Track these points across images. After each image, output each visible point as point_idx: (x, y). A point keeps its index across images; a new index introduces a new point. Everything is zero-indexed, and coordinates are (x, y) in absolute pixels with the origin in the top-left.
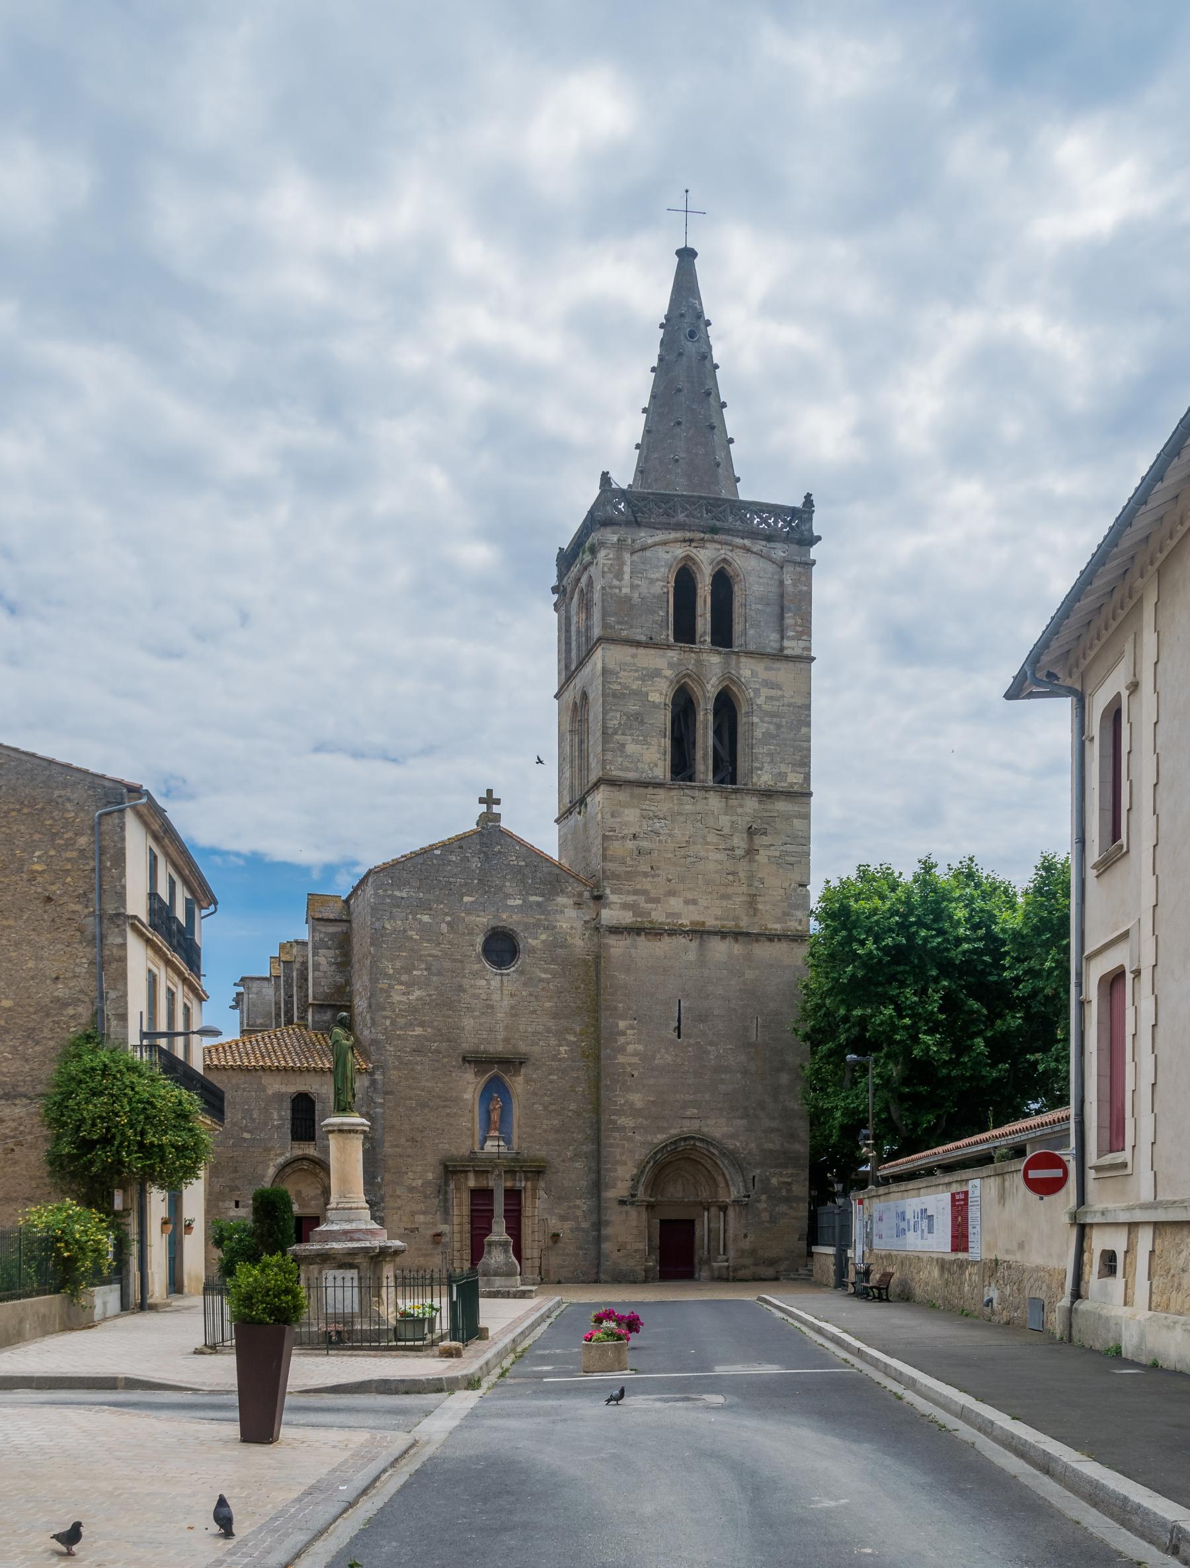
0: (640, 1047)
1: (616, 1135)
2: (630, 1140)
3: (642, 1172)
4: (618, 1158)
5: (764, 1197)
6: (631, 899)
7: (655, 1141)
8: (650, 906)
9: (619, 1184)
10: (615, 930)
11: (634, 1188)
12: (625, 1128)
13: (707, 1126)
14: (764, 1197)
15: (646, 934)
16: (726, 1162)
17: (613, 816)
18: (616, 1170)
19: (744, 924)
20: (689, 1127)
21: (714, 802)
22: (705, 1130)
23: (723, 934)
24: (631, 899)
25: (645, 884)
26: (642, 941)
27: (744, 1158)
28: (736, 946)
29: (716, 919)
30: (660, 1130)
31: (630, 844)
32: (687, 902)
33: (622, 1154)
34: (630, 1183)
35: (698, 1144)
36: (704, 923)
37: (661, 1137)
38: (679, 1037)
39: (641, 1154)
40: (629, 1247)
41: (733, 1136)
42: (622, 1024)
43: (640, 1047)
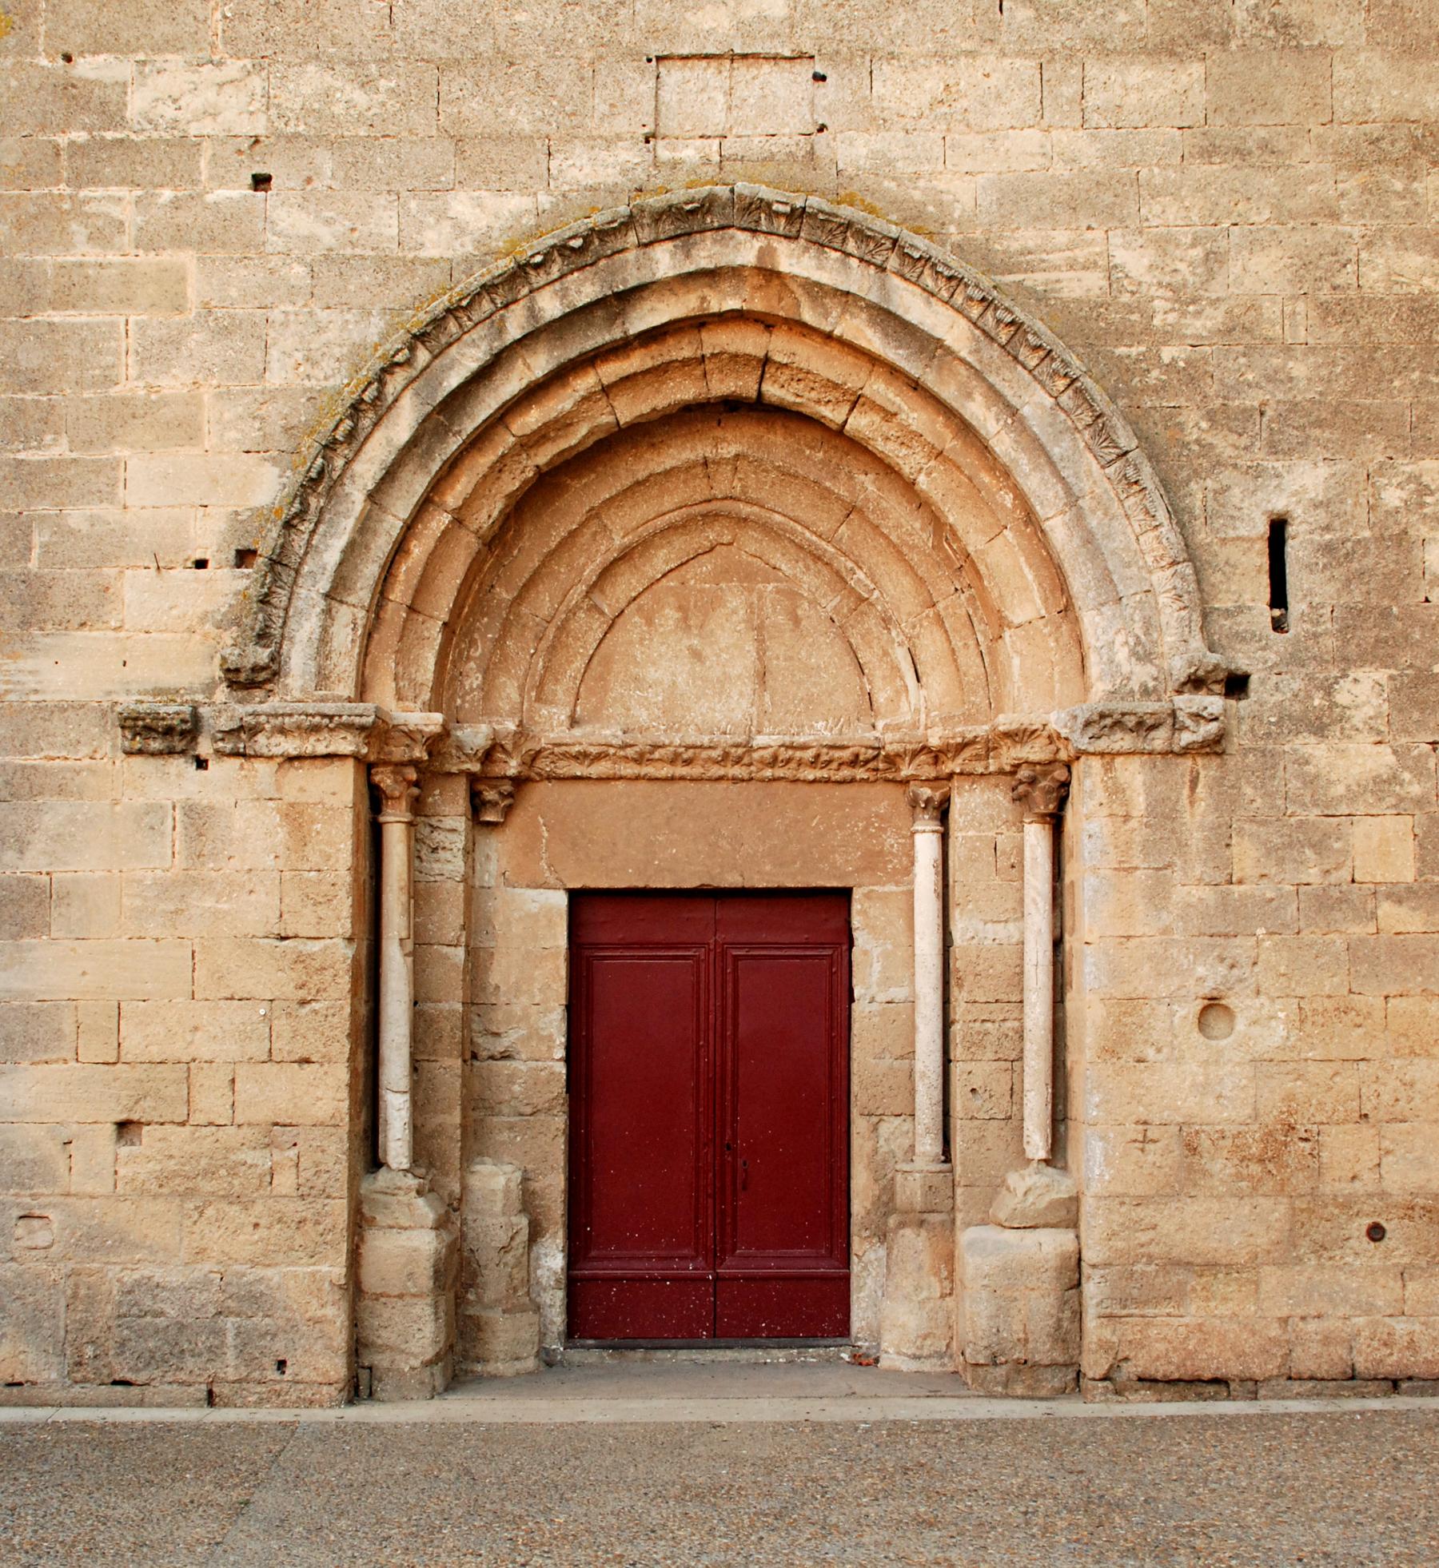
1: (114, 200)
2: (219, 237)
3: (317, 485)
4: (130, 385)
5: (1364, 691)
7: (436, 243)
9: (136, 591)
11: (264, 620)
12: (186, 145)
13: (879, 122)
14: (1364, 691)
16: (1034, 402)
18: (105, 481)
20: (728, 125)
22: (852, 150)
27: (1191, 375)
30: (473, 153)
33: (161, 351)
34: (229, 584)
35: (793, 260)
37: (478, 220)
39: (321, 349)
40: (211, 1102)
41: (1101, 199)
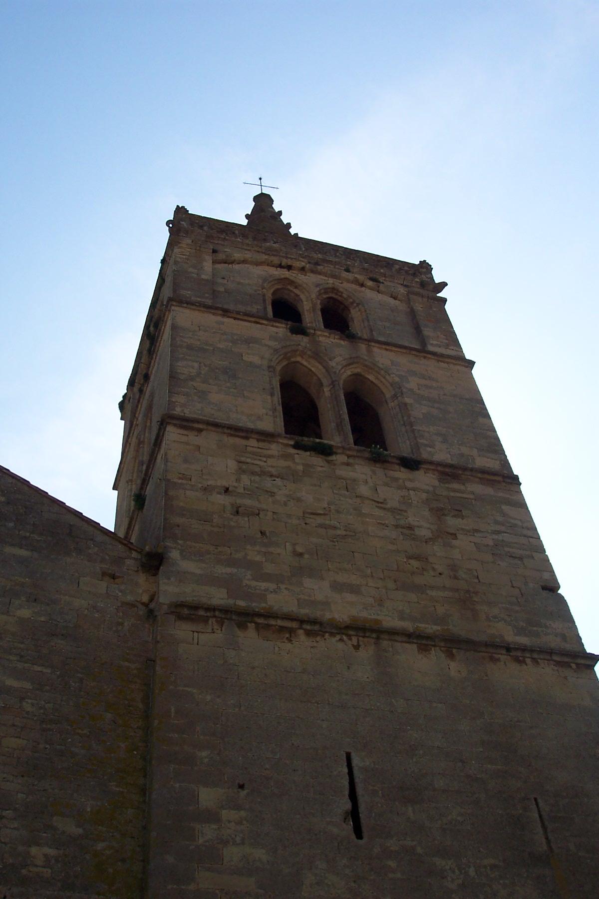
0: (260, 854)
6: (222, 570)
8: (263, 585)
10: (190, 612)
15: (258, 627)
17: (186, 461)
19: (459, 627)
21: (362, 473)
23: (423, 641)
24: (222, 570)
25: (254, 554)
26: (249, 637)
28: (453, 665)
29: (402, 618)
31: (221, 500)
32: (337, 587)
36: (377, 622)
38: (359, 836)
42: (208, 797)
43: (260, 854)
